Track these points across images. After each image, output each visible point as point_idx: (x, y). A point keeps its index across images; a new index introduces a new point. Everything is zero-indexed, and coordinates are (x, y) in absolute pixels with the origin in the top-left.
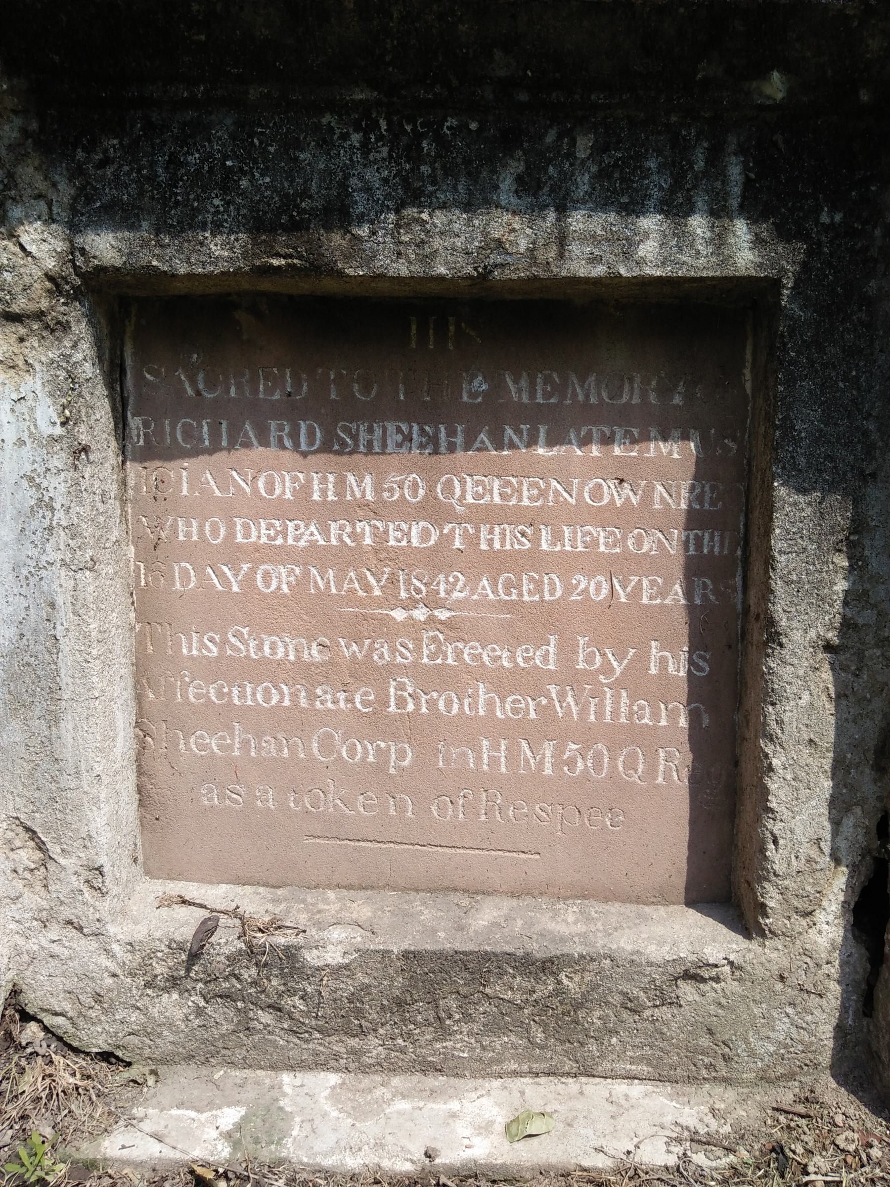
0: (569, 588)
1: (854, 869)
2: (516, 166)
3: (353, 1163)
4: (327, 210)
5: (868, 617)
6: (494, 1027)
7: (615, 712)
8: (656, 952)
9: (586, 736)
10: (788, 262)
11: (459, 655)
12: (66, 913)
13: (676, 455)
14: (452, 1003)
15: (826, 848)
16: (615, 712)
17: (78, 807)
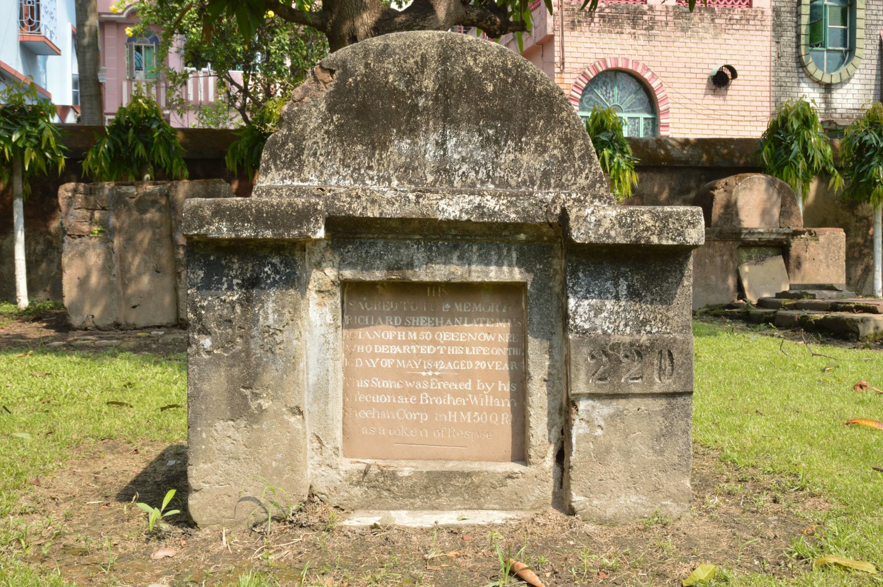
0: (474, 365)
1: (556, 444)
3: (414, 526)
4: (408, 264)
5: (555, 372)
6: (454, 494)
7: (489, 402)
9: (480, 410)
10: (529, 278)
11: (442, 385)
12: (327, 462)
13: (504, 326)
14: (441, 487)
15: (547, 437)
16: (489, 402)
17: (332, 430)
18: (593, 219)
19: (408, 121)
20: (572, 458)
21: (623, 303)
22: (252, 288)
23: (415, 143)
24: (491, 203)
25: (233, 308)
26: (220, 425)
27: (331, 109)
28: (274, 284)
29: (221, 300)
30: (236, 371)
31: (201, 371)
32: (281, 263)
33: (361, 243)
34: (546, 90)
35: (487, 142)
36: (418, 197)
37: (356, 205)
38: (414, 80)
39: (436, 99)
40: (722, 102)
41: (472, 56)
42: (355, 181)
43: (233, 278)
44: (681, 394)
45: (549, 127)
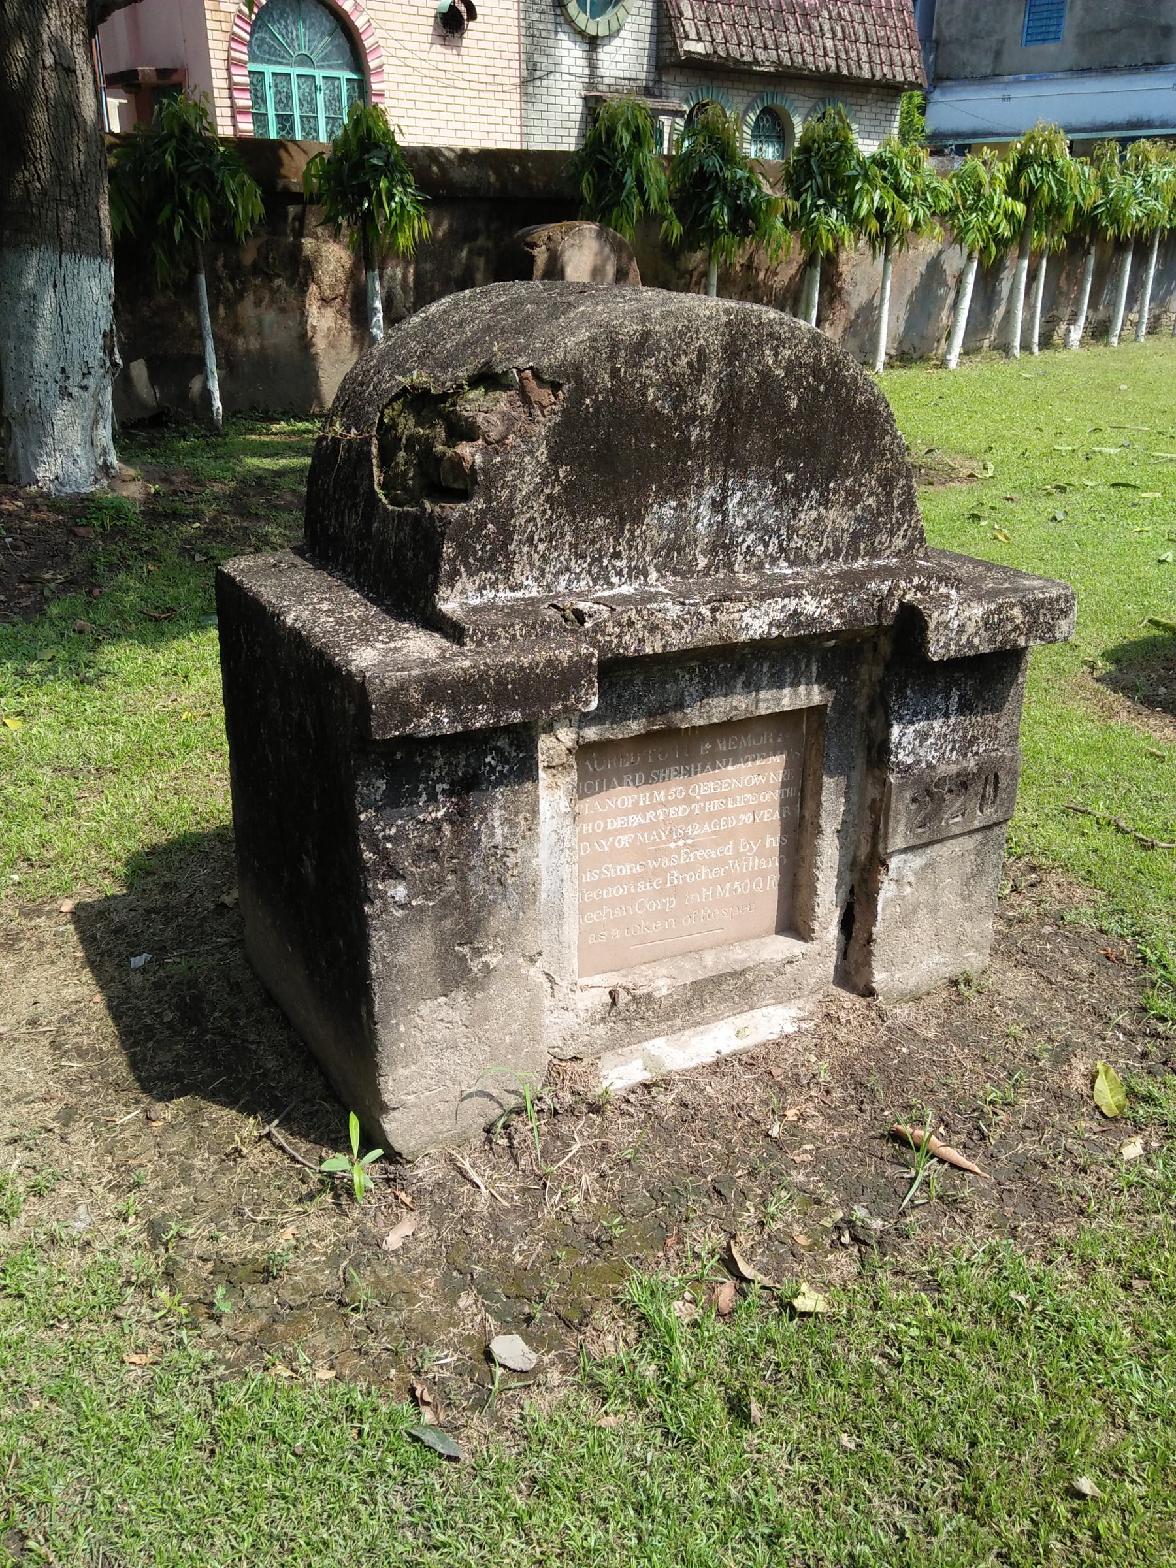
2: (743, 678)
3: (693, 1064)
8: (779, 957)
10: (830, 696)
12: (562, 1004)
13: (778, 761)
18: (956, 623)
19: (673, 469)
20: (875, 930)
21: (952, 720)
22: (468, 792)
23: (682, 506)
24: (811, 606)
25: (439, 829)
26: (425, 1008)
27: (555, 457)
28: (502, 780)
29: (418, 821)
30: (447, 924)
31: (392, 938)
32: (511, 745)
33: (611, 683)
34: (869, 401)
35: (784, 495)
36: (713, 610)
37: (627, 638)
38: (685, 396)
39: (716, 427)
40: (455, 59)
41: (771, 349)
42: (595, 581)
43: (435, 782)
44: (997, 824)
45: (865, 466)
